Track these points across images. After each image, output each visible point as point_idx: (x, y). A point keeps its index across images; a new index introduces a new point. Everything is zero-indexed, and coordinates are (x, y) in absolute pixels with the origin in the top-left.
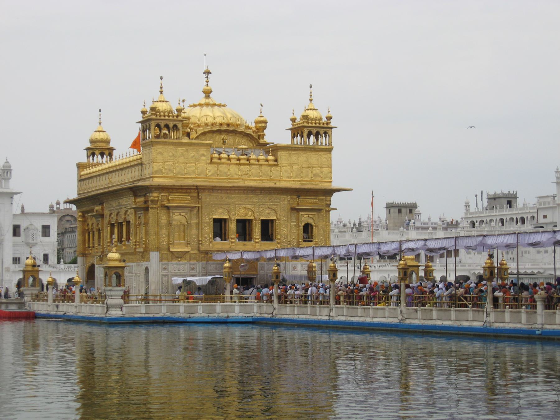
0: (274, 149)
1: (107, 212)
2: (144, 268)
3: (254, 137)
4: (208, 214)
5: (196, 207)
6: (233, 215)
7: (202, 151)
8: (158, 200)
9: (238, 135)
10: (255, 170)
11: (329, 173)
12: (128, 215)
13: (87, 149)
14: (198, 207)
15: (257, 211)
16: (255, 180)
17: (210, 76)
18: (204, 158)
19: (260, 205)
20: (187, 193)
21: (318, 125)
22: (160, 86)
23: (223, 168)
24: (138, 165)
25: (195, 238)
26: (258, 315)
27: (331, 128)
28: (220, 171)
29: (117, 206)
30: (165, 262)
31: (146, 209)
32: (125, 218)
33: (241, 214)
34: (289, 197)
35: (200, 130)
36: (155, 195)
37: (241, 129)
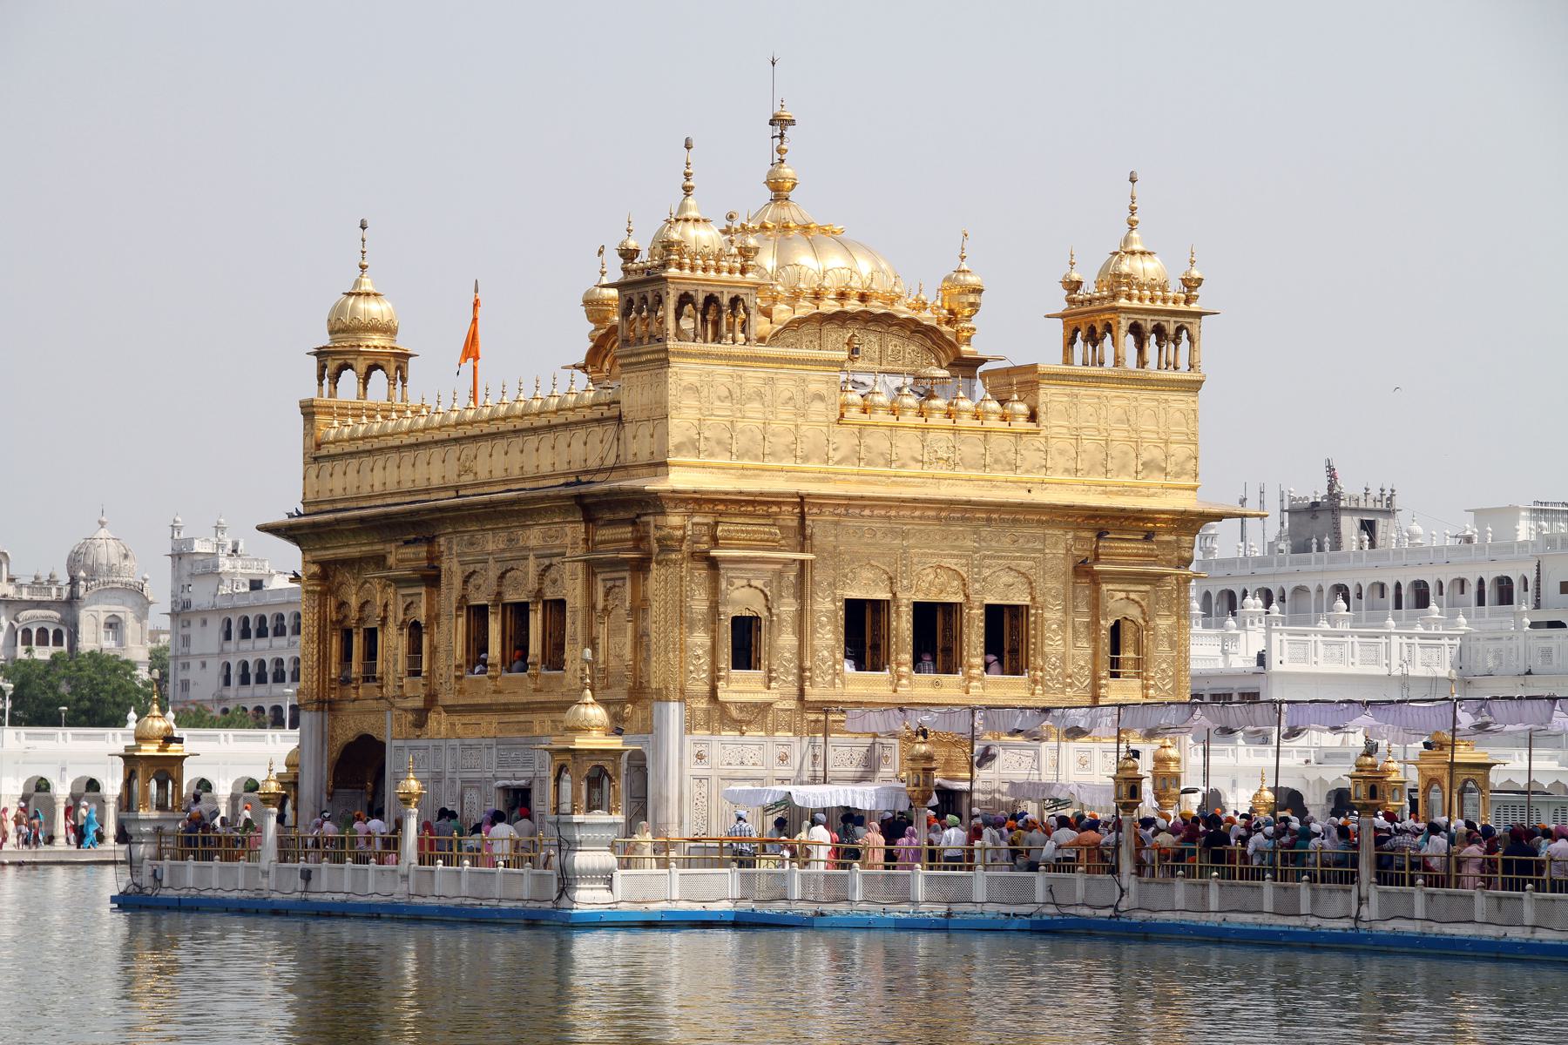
1: (452, 567)
4: (833, 585)
8: (683, 538)
11: (1189, 458)
12: (554, 582)
13: (321, 354)
14: (802, 562)
15: (983, 581)
17: (790, 131)
18: (818, 406)
19: (985, 557)
20: (769, 516)
21: (1159, 305)
22: (683, 168)
24: (600, 421)
25: (790, 661)
26: (1051, 910)
28: (868, 448)
29: (503, 550)
30: (701, 734)
31: (640, 567)
32: (540, 590)
34: (1070, 535)
35: (783, 313)
37: (902, 310)
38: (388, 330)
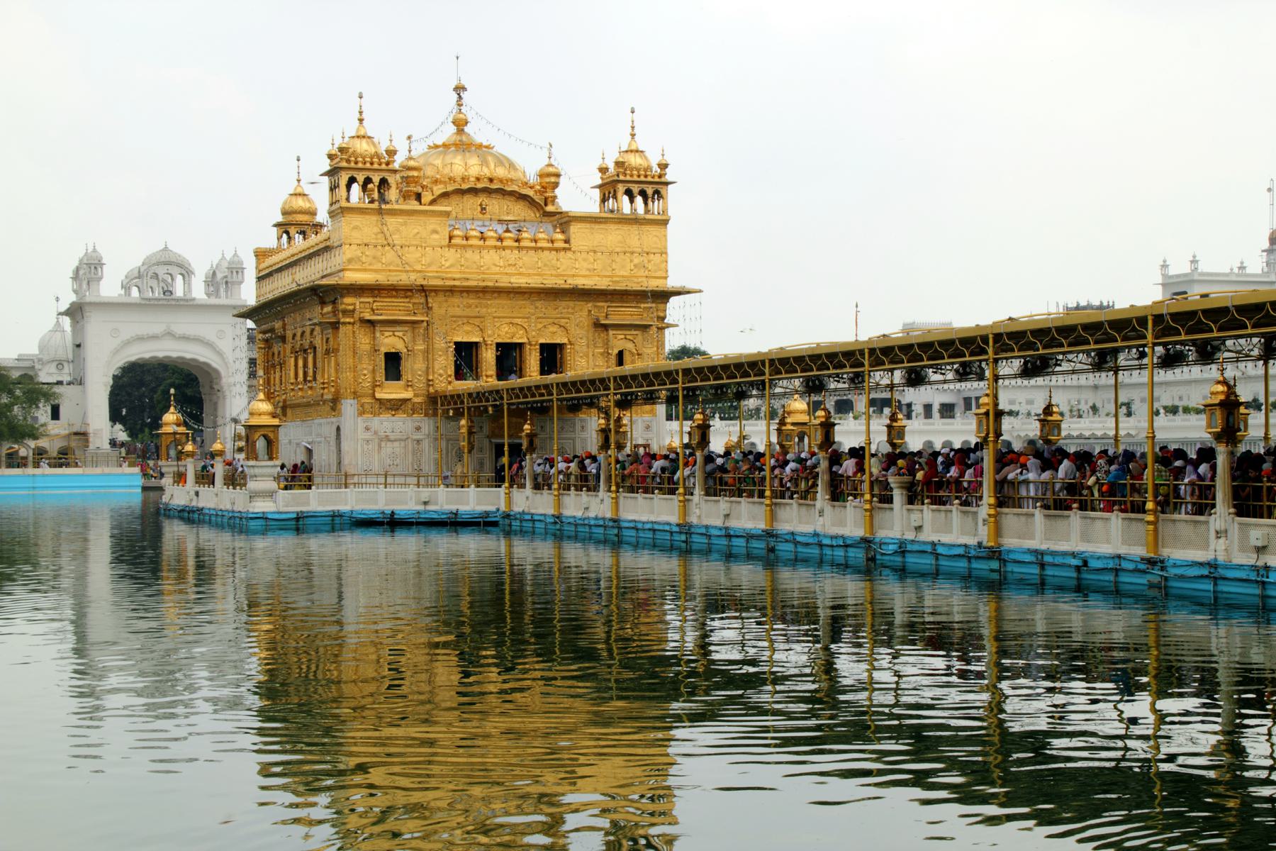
0: (564, 221)
2: (334, 428)
3: (538, 200)
7: (433, 223)
8: (353, 311)
10: (529, 258)
13: (278, 225)
16: (529, 275)
18: (435, 236)
21: (642, 179)
23: (469, 254)
27: (667, 184)
28: (466, 260)
31: (335, 326)
33: (506, 334)
34: (590, 305)
35: (439, 189)
36: (348, 300)
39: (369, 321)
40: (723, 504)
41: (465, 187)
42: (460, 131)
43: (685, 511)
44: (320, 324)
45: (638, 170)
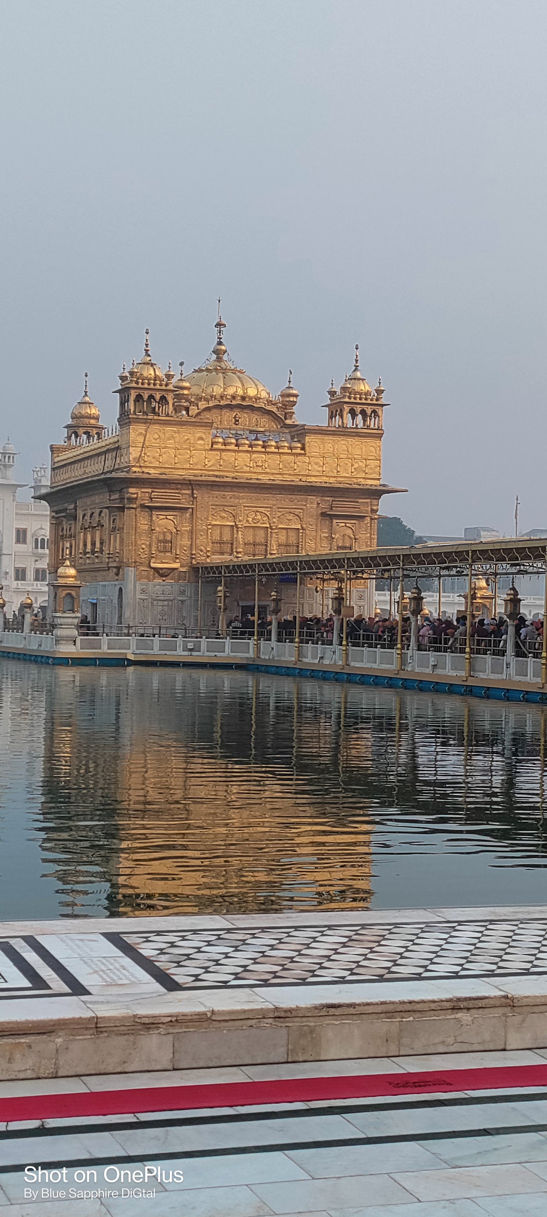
2: (117, 588)
5: (189, 508)
6: (240, 521)
7: (200, 432)
8: (136, 499)
9: (256, 412)
11: (376, 467)
13: (68, 427)
14: (192, 508)
19: (278, 508)
21: (363, 401)
23: (229, 457)
25: (185, 550)
31: (122, 509)
35: (203, 405)
36: (132, 490)
38: (97, 418)
39: (148, 507)
40: (432, 657)
41: (222, 403)
42: (219, 359)
43: (403, 661)
44: (107, 508)
45: (360, 394)
